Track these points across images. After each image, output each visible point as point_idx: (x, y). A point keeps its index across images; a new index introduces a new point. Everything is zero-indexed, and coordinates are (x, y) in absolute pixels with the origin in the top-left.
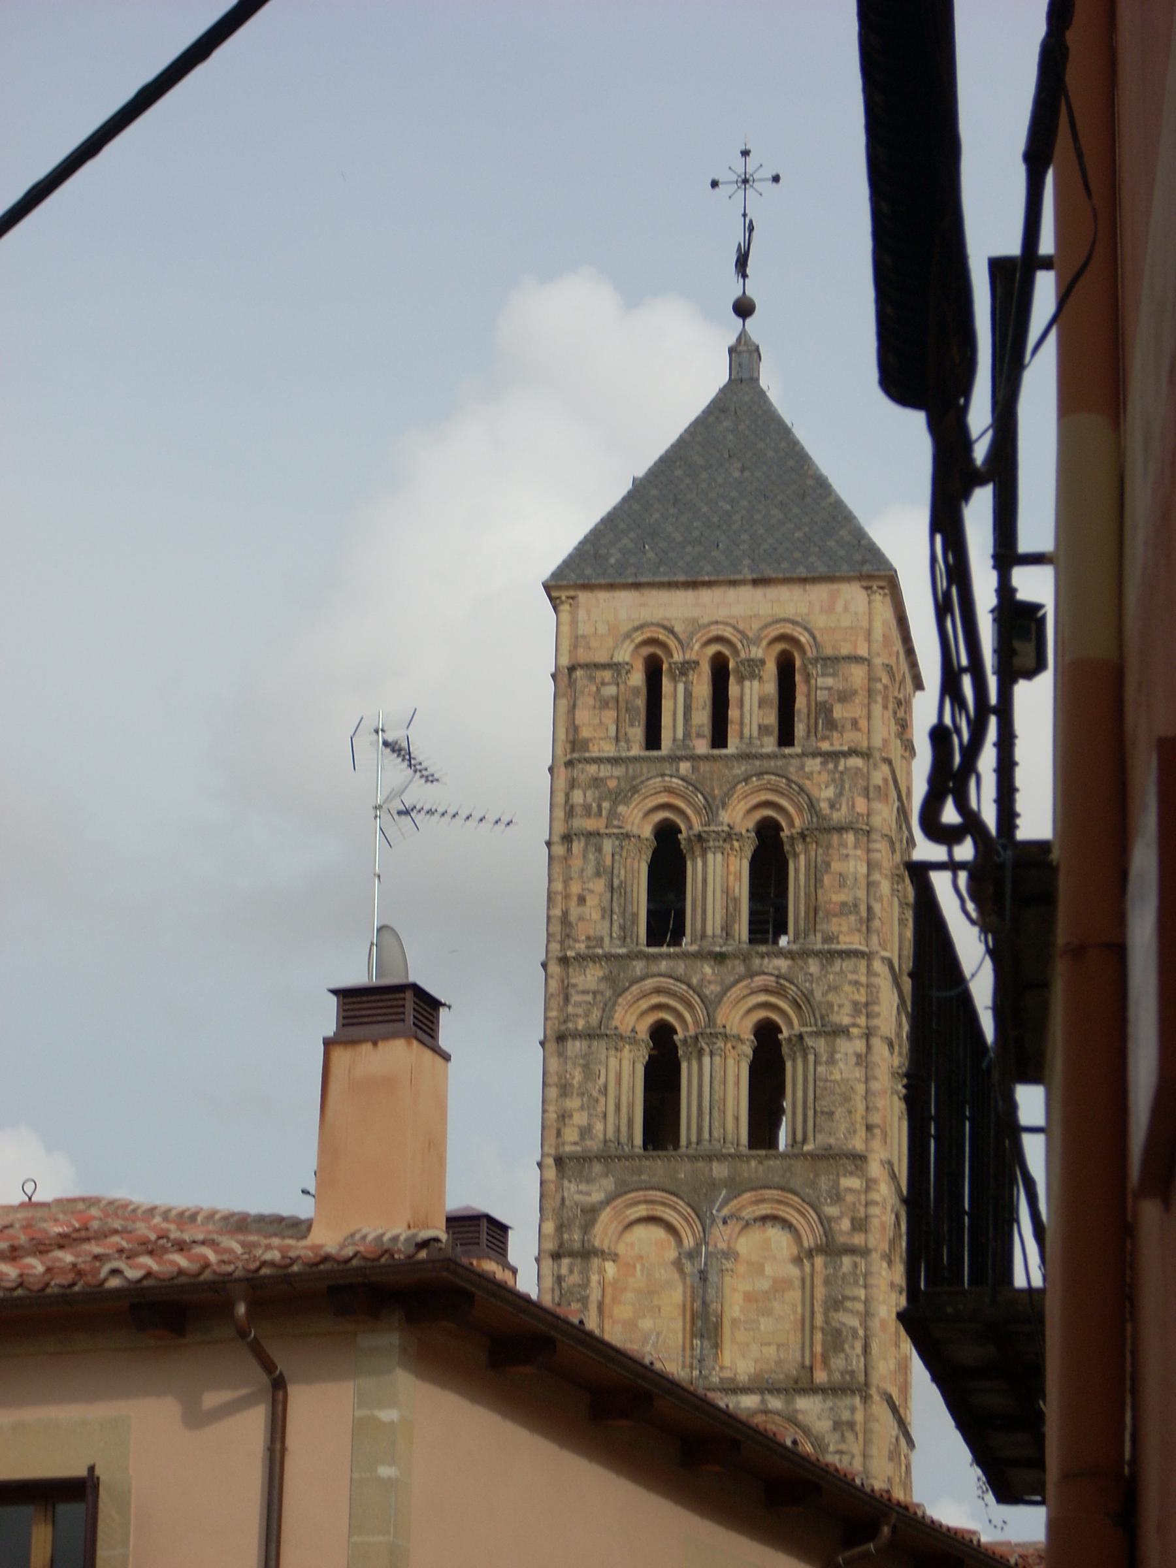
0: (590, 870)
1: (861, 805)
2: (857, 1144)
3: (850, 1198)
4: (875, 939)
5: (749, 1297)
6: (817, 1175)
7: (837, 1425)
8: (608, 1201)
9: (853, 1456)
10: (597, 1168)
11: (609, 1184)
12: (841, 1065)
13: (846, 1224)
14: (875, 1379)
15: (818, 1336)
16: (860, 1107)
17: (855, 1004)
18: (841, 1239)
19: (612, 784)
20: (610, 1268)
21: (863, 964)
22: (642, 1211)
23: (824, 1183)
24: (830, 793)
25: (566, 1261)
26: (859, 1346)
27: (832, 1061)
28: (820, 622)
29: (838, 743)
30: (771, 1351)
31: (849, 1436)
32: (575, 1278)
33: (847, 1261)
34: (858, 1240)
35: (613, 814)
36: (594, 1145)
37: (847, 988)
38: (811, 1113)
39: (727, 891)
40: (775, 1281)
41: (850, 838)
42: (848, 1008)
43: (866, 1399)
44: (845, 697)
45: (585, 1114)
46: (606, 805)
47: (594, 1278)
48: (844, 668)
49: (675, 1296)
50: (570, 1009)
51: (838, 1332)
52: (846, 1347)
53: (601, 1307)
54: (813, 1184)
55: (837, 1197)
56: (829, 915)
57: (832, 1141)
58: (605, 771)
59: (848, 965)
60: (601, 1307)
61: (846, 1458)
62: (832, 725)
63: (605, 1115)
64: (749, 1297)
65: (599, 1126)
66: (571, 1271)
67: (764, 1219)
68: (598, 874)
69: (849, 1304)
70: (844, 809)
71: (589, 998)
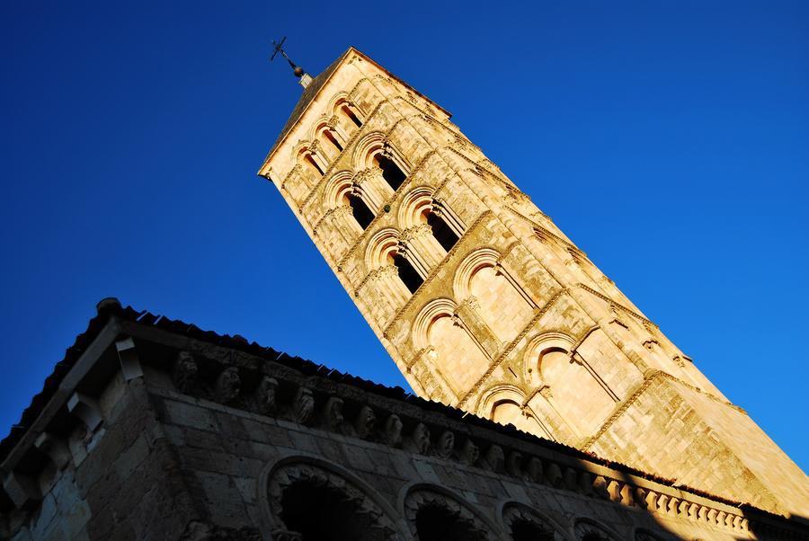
0: (327, 232)
1: (396, 114)
2: (483, 208)
4: (433, 144)
5: (492, 309)
7: (564, 315)
9: (583, 319)
10: (399, 322)
11: (407, 323)
12: (455, 192)
13: (502, 239)
14: (564, 282)
15: (527, 290)
16: (475, 197)
17: (443, 168)
18: (505, 247)
19: (316, 202)
20: (433, 354)
21: (436, 155)
22: (428, 320)
23: (482, 235)
24: (383, 122)
25: (413, 369)
26: (547, 276)
27: (450, 194)
28: (343, 87)
29: (373, 108)
30: (518, 317)
31: (573, 313)
32: (421, 370)
33: (514, 252)
34: (512, 240)
35: (322, 209)
36: (392, 316)
38: (458, 219)
39: (378, 190)
40: (497, 291)
41: (399, 126)
42: (441, 172)
43: (568, 292)
44: (366, 95)
45: (382, 310)
46: (319, 209)
47: (427, 363)
48: (360, 88)
49: (464, 337)
50: (352, 282)
51: (534, 279)
52: (541, 281)
53: (438, 371)
54: (478, 240)
55: (491, 234)
56: (411, 155)
57: (472, 218)
58: (311, 201)
59: (430, 160)
60: (438, 371)
61: (580, 323)
62: (368, 106)
64: (492, 309)
65: (389, 308)
66: (418, 370)
67: (473, 274)
68: (331, 231)
69: (528, 265)
70: (391, 122)
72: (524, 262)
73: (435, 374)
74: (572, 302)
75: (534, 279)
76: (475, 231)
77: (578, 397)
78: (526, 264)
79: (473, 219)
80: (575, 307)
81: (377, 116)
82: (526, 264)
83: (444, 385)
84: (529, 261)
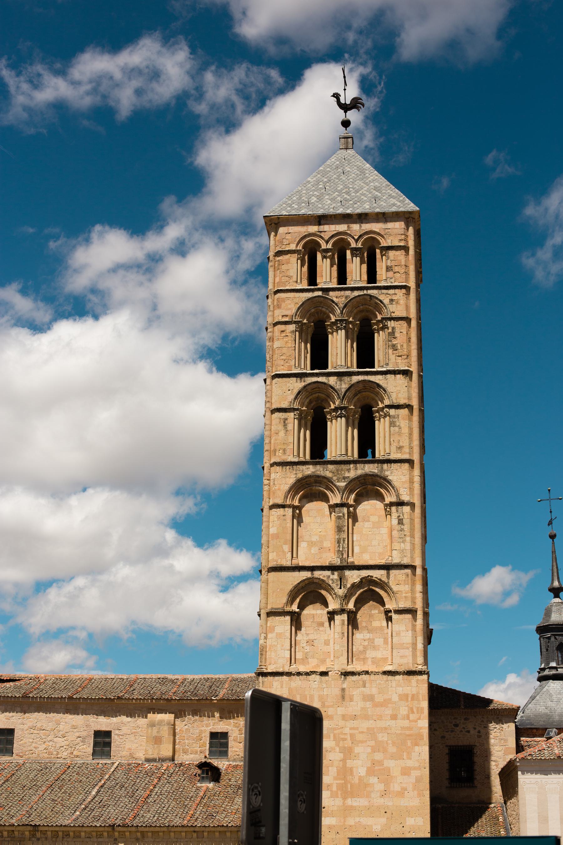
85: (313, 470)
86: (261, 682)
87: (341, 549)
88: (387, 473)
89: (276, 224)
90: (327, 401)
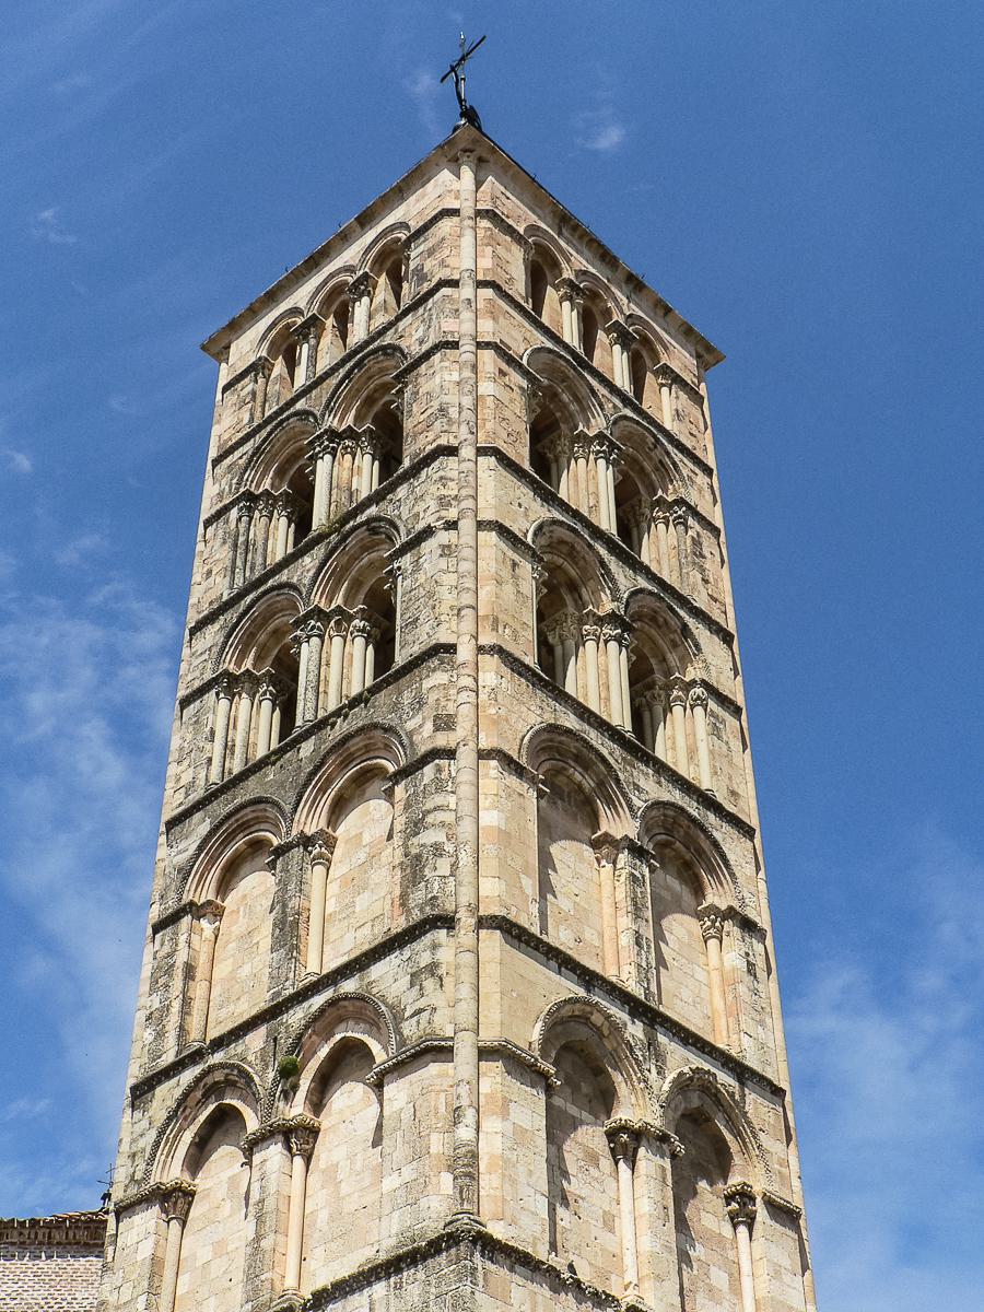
3: (432, 698)
6: (400, 693)
8: (200, 849)
22: (239, 843)
31: (430, 984)
34: (442, 740)
37: (433, 489)
56: (415, 437)
63: (210, 760)
69: (430, 819)
71: (206, 656)
72: (429, 805)
73: (179, 974)
74: (445, 956)
75: (418, 857)
76: (403, 681)
77: (345, 1188)
78: (429, 812)
79: (416, 650)
80: (442, 971)
81: (421, 310)
82: (429, 812)
83: (176, 1006)
84: (436, 809)
85: (578, 727)
86: (480, 1268)
87: (644, 964)
88: (717, 835)
89: (481, 160)
90: (573, 588)
